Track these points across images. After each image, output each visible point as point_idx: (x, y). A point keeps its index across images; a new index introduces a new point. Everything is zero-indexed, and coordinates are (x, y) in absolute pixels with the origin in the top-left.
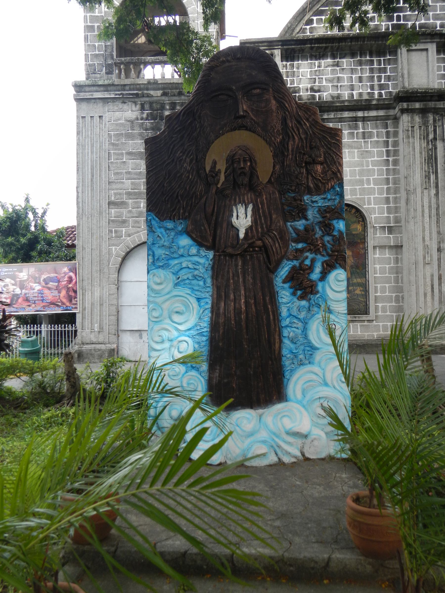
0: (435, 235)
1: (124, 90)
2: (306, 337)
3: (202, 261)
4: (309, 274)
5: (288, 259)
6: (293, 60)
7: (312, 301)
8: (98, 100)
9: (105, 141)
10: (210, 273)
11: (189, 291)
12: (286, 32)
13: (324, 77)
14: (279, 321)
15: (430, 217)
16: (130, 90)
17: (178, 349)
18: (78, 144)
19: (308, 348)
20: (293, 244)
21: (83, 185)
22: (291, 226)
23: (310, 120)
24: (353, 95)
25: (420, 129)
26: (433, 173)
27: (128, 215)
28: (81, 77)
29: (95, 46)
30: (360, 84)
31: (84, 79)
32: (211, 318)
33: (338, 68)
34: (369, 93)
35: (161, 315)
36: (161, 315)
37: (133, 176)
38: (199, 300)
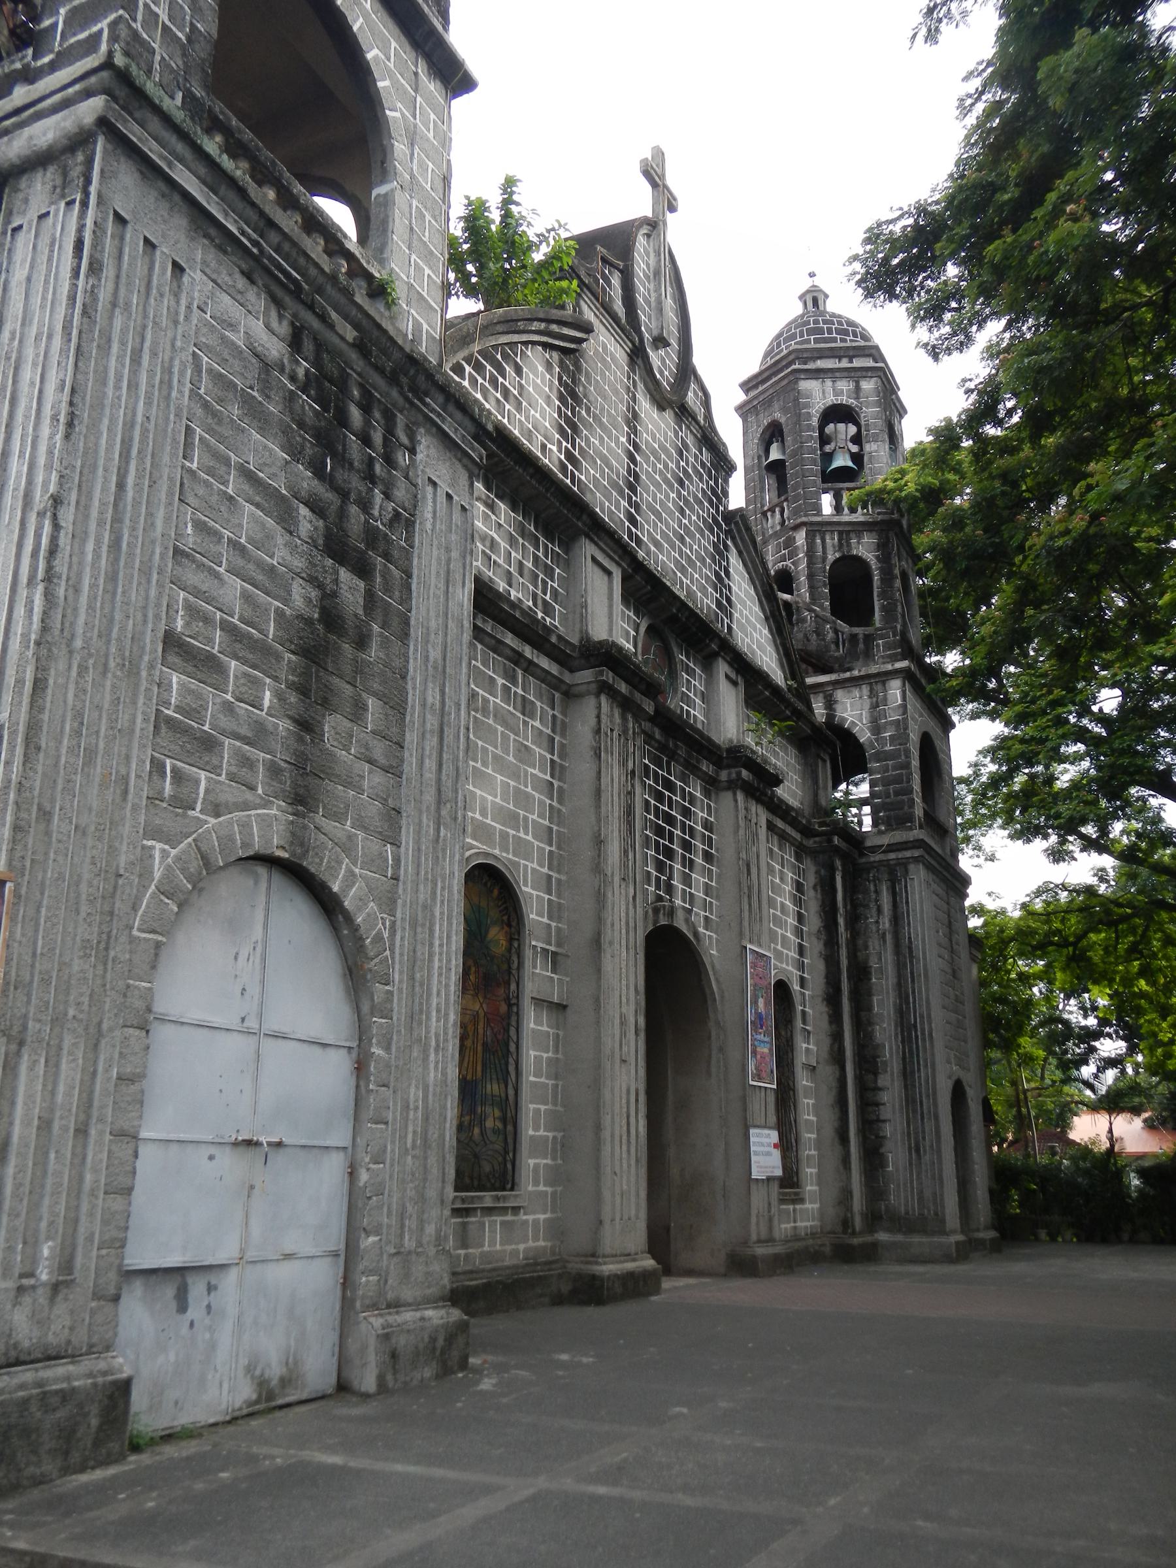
8: (177, 198)
27: (225, 722)
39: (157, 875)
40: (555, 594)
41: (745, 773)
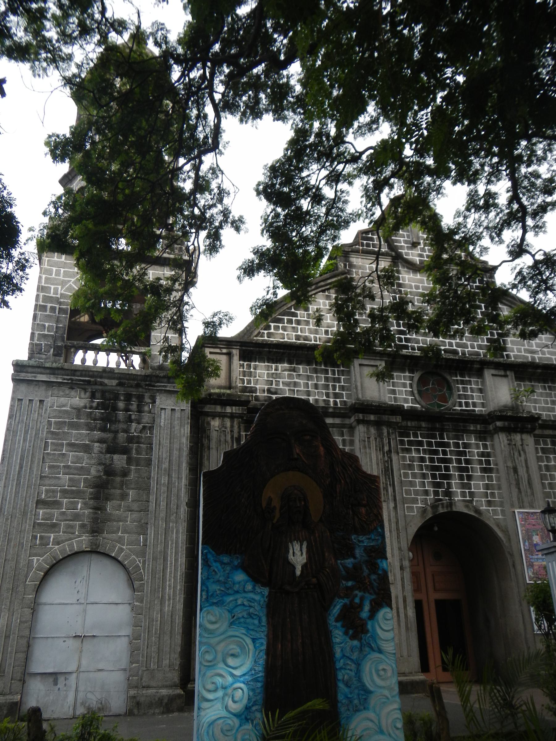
0: (396, 552)
1: (74, 375)
2: (360, 679)
3: (257, 598)
4: (359, 612)
5: (340, 597)
6: (250, 361)
7: (363, 641)
8: (40, 383)
9: (43, 428)
10: (265, 610)
11: (244, 632)
12: (245, 334)
13: (281, 380)
14: (334, 663)
15: (390, 531)
16: (81, 376)
17: (233, 698)
18: (8, 429)
19: (362, 692)
20: (344, 582)
21: (6, 478)
22: (341, 564)
23: (353, 466)
25: (376, 441)
26: (390, 485)
27: (60, 518)
28: (24, 356)
29: (44, 326)
30: (316, 391)
31: (26, 359)
32: (267, 661)
33: (295, 374)
34: (324, 400)
35: (215, 658)
36: (215, 658)
37: (72, 471)
38: (254, 640)
39: (35, 566)
40: (342, 388)
41: (499, 424)
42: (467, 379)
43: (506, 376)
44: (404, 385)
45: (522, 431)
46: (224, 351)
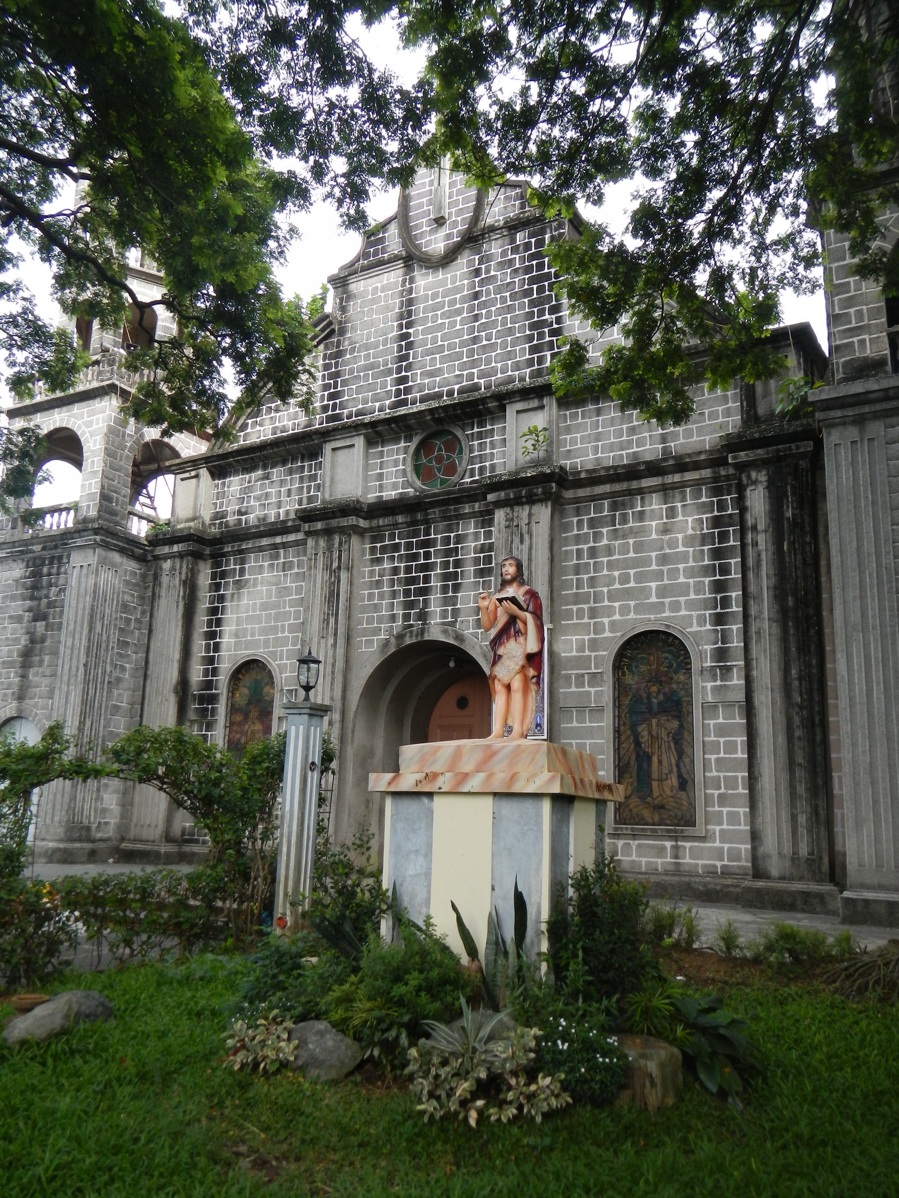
6: (225, 478)
24: (279, 514)
42: (489, 427)
43: (542, 407)
44: (396, 463)
45: (531, 500)
46: (193, 473)
